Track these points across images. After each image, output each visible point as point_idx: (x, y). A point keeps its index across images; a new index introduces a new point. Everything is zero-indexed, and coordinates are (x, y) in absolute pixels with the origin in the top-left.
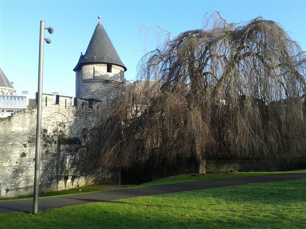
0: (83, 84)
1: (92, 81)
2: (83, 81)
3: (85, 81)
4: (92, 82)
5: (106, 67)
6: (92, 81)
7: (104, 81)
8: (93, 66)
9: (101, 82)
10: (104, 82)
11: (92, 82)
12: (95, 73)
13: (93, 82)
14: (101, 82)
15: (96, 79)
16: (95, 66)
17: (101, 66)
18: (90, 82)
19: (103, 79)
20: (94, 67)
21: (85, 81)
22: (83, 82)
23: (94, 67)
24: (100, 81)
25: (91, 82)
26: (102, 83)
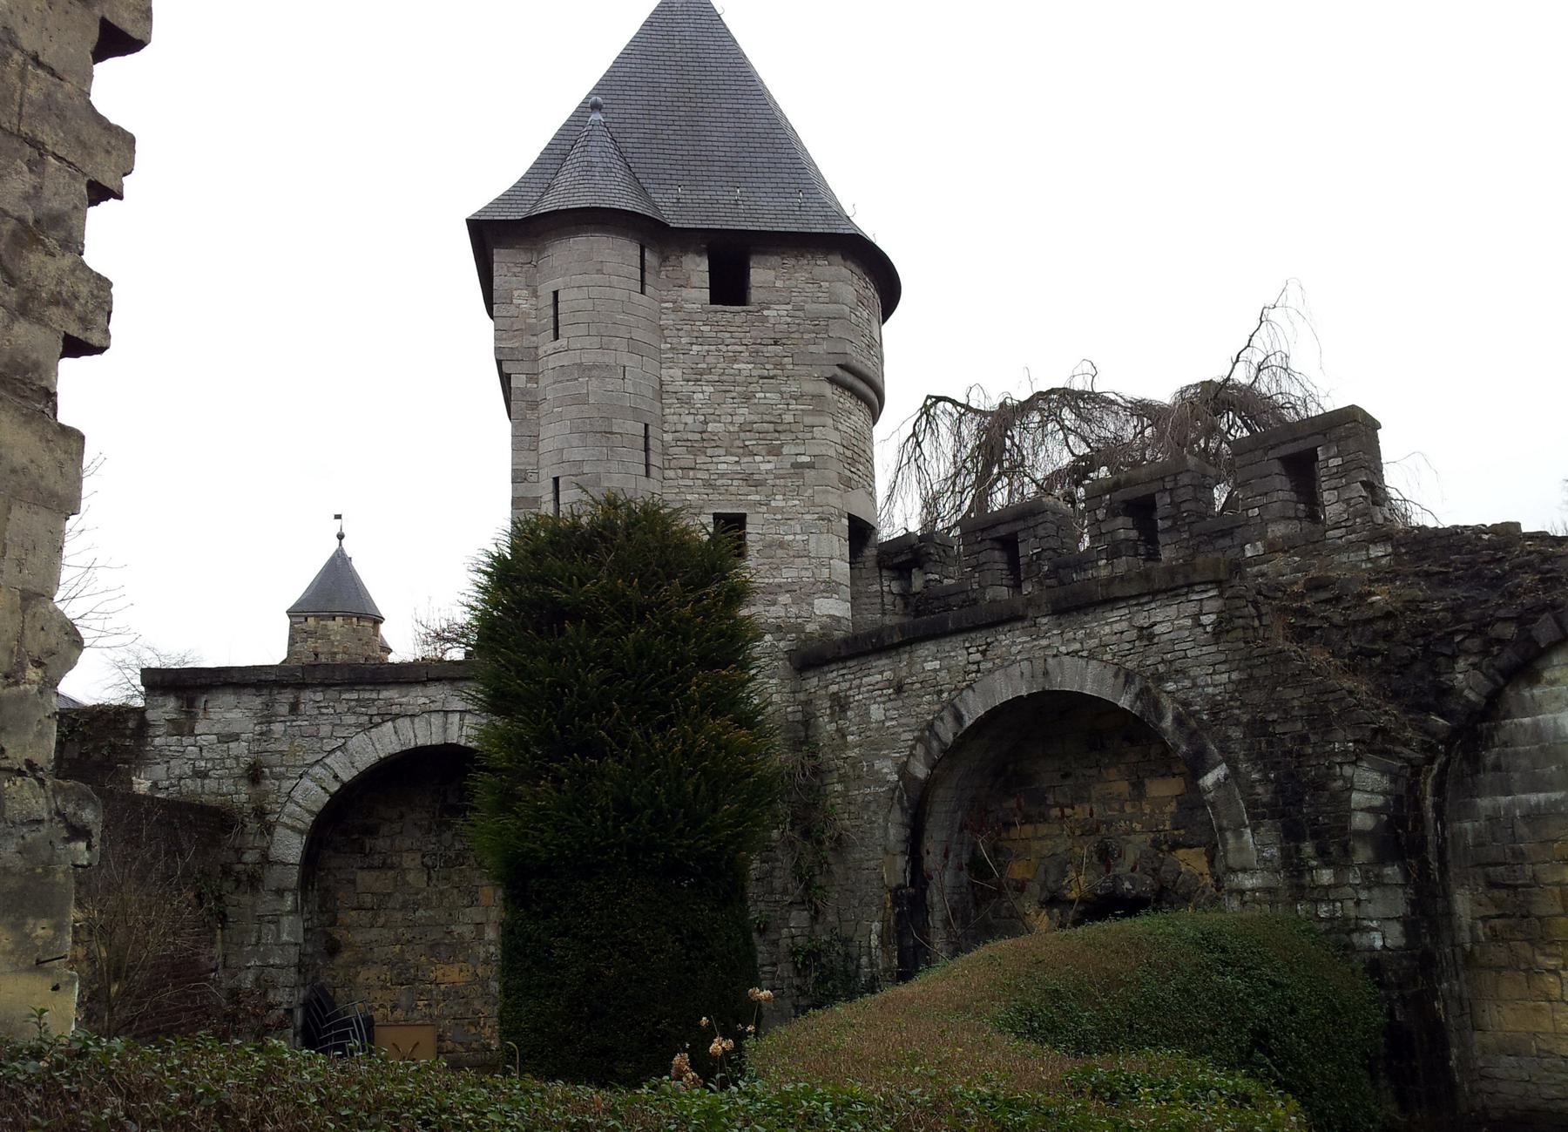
0: (828, 389)
3: (849, 378)
21: (849, 378)
22: (832, 380)
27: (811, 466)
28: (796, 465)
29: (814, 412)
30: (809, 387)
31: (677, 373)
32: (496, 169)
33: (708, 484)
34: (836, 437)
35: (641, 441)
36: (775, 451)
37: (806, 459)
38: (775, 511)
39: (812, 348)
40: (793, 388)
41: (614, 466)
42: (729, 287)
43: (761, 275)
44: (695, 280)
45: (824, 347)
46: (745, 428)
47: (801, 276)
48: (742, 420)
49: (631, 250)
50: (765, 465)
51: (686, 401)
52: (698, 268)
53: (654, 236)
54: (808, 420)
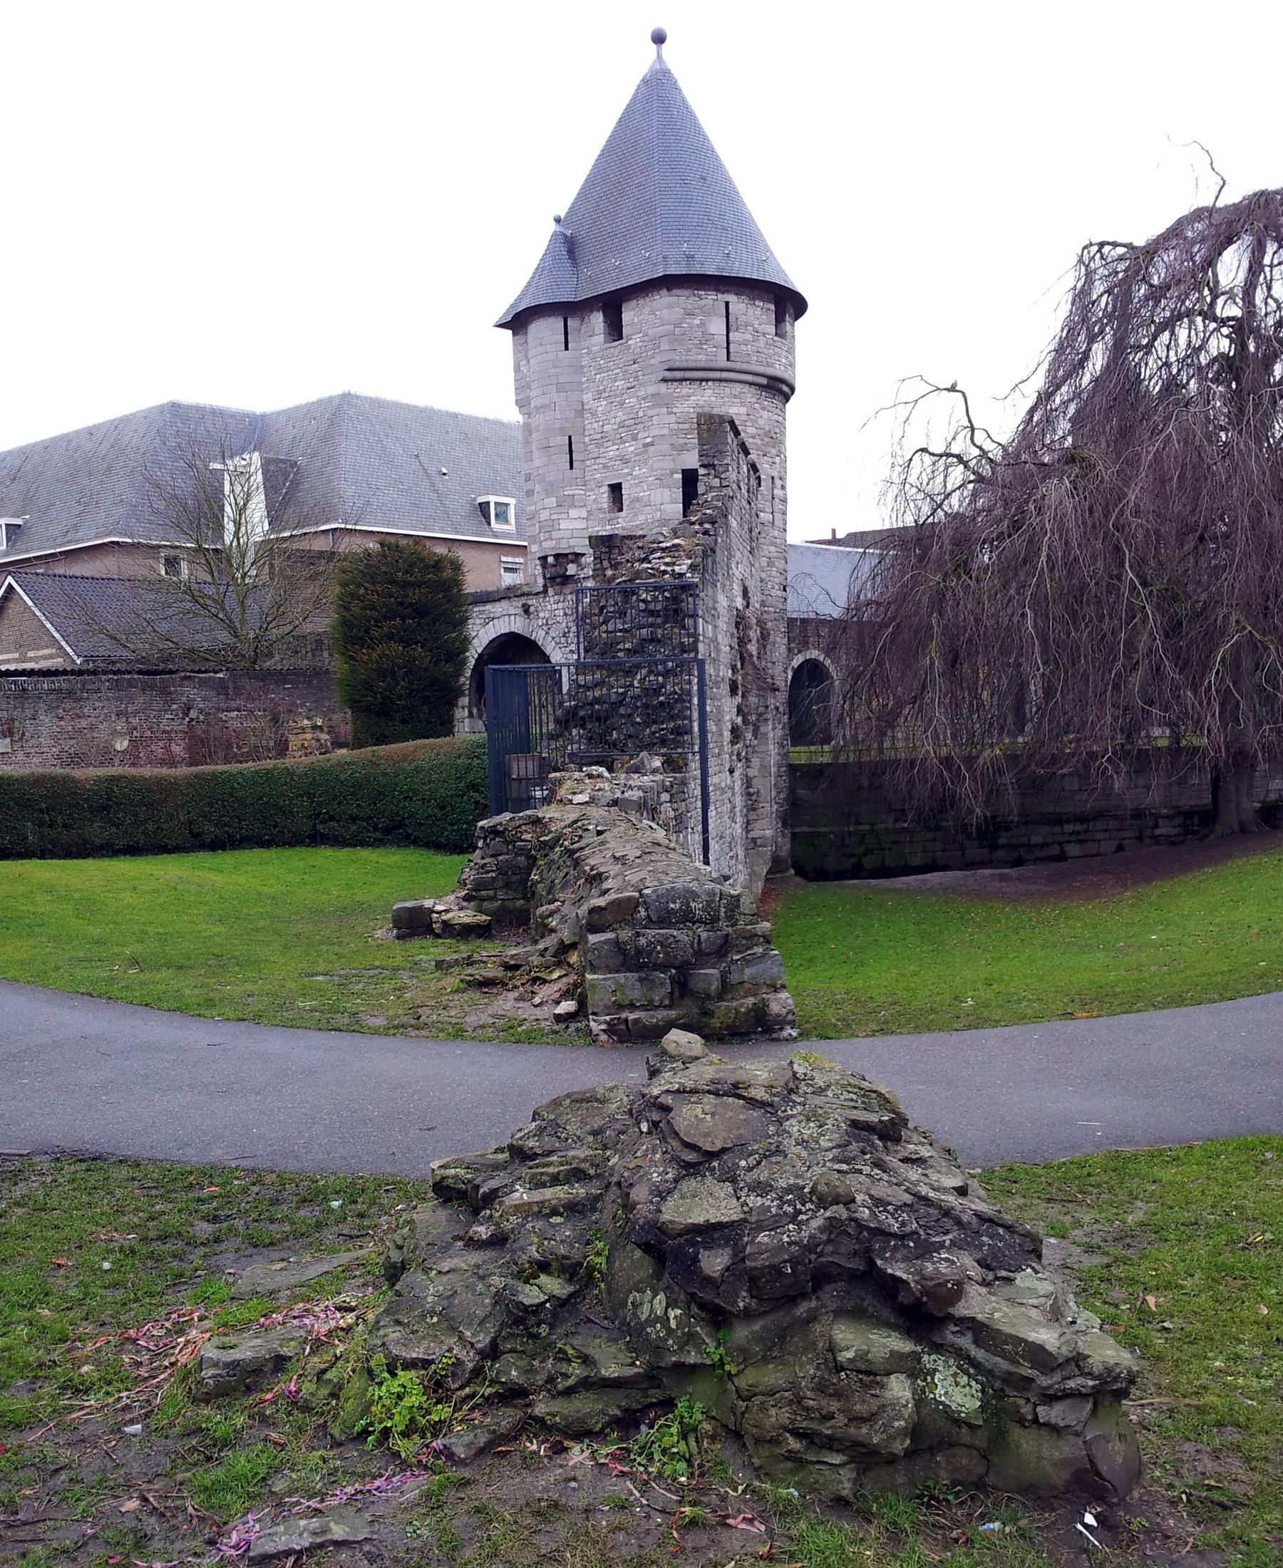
0: (663, 388)
1: (717, 375)
2: (668, 375)
3: (679, 375)
4: (713, 380)
5: (772, 307)
6: (717, 375)
7: (764, 381)
8: (720, 296)
9: (751, 384)
10: (760, 385)
11: (713, 380)
12: (731, 334)
13: (720, 380)
14: (751, 384)
15: (738, 366)
16: (732, 298)
17: (754, 299)
18: (702, 380)
19: (761, 369)
20: (727, 303)
21: (679, 375)
22: (665, 380)
23: (727, 303)
24: (750, 378)
25: (707, 380)
26: (753, 389)
27: (652, 444)
28: (646, 445)
29: (653, 407)
30: (651, 389)
31: (590, 395)
32: (509, 289)
33: (605, 467)
34: (672, 418)
35: (567, 448)
36: (635, 438)
37: (649, 440)
38: (637, 477)
39: (652, 361)
40: (642, 393)
41: (551, 467)
42: (615, 330)
43: (627, 316)
44: (597, 331)
45: (658, 358)
46: (621, 425)
47: (647, 310)
48: (618, 420)
49: (557, 323)
50: (631, 448)
51: (594, 414)
52: (597, 320)
53: (567, 310)
54: (650, 413)
